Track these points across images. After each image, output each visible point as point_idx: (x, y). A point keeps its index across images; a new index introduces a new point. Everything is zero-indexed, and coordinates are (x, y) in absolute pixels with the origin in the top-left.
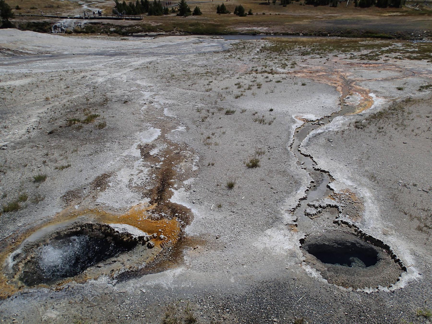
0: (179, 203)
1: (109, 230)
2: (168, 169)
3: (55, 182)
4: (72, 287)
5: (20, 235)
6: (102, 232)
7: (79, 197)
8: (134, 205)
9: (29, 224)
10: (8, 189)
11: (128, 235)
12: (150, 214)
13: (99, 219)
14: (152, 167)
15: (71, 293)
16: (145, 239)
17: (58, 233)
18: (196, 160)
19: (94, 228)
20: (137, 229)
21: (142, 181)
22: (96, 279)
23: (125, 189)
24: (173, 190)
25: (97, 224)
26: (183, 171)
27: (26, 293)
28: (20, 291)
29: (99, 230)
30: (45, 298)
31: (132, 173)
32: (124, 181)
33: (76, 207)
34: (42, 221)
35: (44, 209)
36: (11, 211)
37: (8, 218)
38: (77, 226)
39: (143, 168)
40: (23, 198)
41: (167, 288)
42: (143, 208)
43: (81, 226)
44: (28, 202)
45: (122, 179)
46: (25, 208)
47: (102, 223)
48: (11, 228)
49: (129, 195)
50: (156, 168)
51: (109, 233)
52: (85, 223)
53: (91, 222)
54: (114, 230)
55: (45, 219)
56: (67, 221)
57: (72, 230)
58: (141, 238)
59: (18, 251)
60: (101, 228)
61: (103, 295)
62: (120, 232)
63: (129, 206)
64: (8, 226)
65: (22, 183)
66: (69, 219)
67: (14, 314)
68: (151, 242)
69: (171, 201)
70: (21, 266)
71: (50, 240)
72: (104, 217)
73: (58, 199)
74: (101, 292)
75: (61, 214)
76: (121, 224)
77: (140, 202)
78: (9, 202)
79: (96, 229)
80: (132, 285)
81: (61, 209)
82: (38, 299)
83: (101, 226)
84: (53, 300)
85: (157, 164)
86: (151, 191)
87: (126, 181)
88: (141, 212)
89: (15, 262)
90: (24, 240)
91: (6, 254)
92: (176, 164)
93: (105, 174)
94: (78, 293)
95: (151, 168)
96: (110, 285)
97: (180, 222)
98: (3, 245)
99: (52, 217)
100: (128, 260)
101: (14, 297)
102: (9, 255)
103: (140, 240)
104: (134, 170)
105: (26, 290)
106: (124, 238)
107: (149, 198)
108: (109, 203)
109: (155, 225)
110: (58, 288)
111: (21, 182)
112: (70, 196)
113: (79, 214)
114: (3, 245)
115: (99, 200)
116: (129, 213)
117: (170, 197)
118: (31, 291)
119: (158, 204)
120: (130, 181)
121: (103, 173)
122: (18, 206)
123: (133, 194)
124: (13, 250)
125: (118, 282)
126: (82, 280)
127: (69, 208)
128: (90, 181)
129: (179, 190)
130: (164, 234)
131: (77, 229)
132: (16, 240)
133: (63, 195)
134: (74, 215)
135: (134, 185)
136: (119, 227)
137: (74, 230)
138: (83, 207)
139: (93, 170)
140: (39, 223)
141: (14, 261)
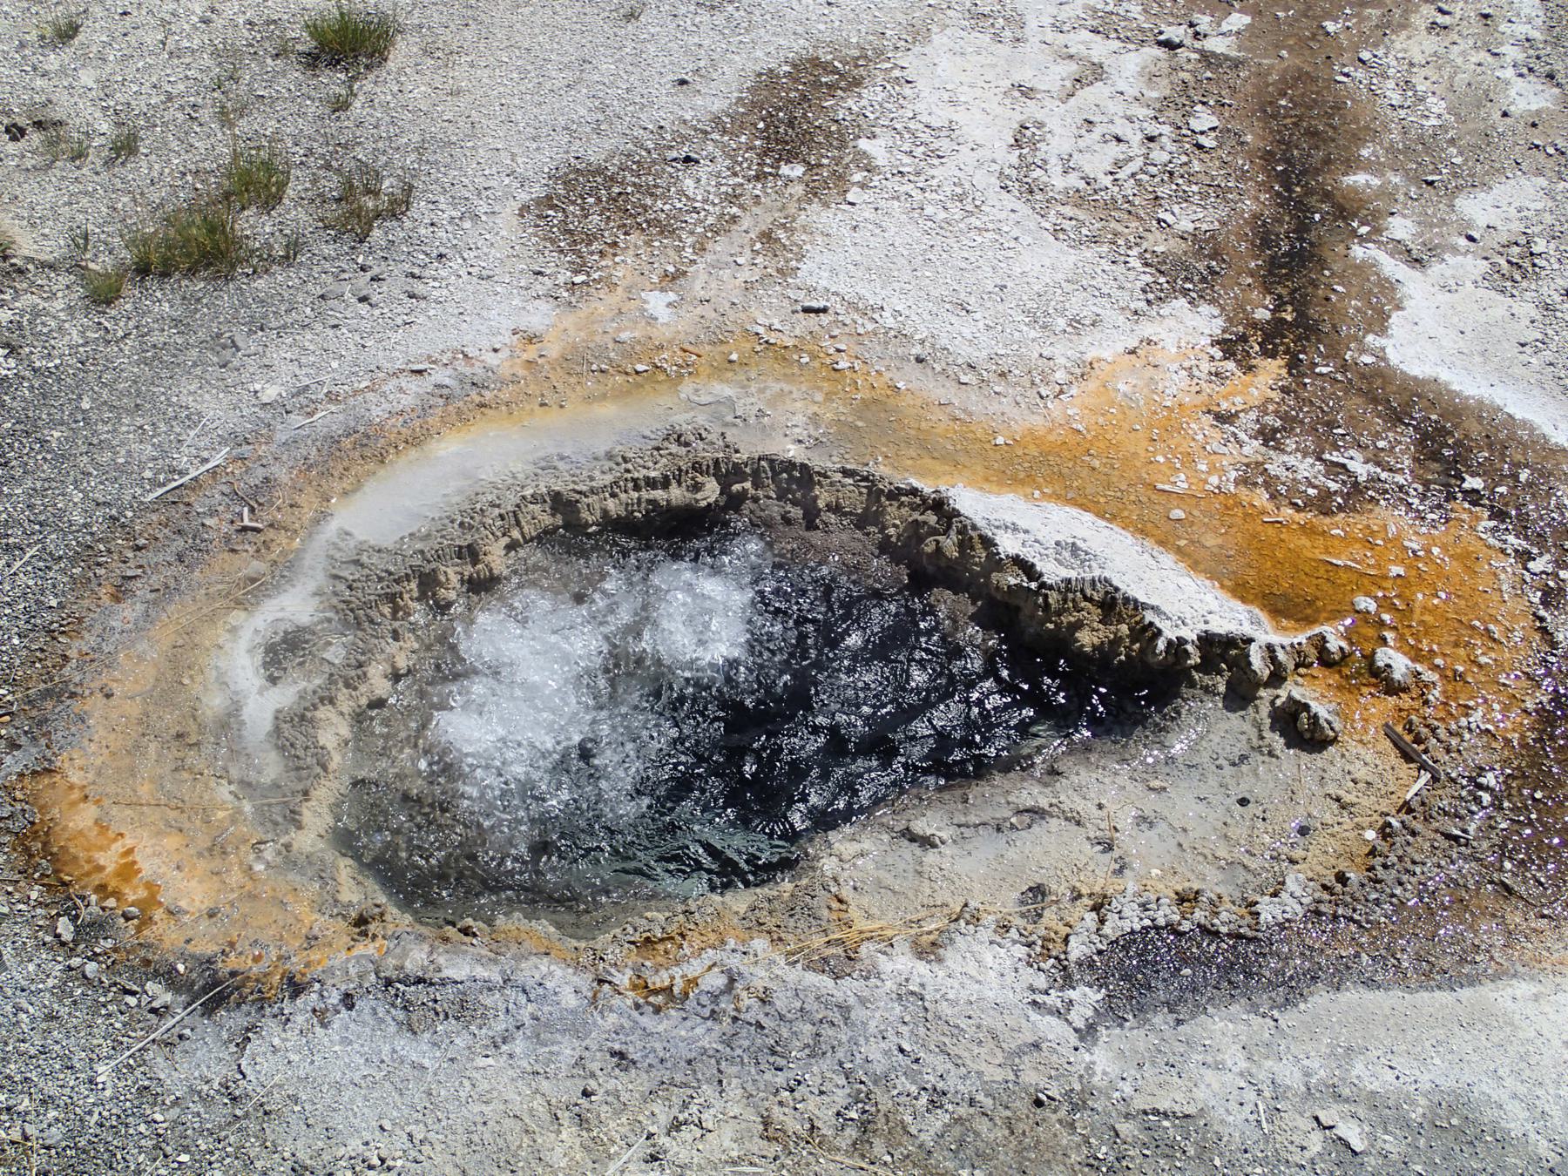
0: (1468, 384)
1: (950, 544)
2: (1301, 76)
3: (460, 75)
4: (759, 984)
5: (281, 473)
6: (885, 547)
7: (666, 230)
8: (1106, 346)
9: (332, 397)
10: (139, 96)
11: (1112, 604)
12: (1253, 448)
13: (846, 432)
14: (1169, 45)
15: (759, 1039)
16: (1257, 661)
17: (558, 502)
18: (1522, 29)
19: (823, 497)
20: (1168, 559)
21: (1114, 150)
22: (929, 950)
23: (1003, 207)
24: (1392, 267)
25: (846, 473)
26: (1436, 105)
27: (420, 981)
28: (367, 949)
29: (861, 522)
30: (567, 1050)
31: (1025, 76)
32: (978, 135)
33: (657, 303)
34: (427, 384)
35: (419, 288)
36: (192, 272)
37: (176, 322)
38: (696, 467)
39: (1100, 49)
40: (256, 183)
41: (1543, 1148)
42: (1175, 384)
43: (728, 474)
44: (295, 214)
45: (960, 117)
46: (287, 260)
47: (886, 472)
48: (215, 409)
49: (1044, 260)
50: (1207, 57)
51: (934, 559)
52: (749, 447)
53: (793, 452)
54: (988, 542)
55: (441, 376)
56: (607, 410)
57: (658, 494)
58: (1221, 650)
59: (296, 605)
60: (881, 513)
61: (1022, 1106)
62: (1052, 572)
63: (1063, 353)
64: (186, 392)
65: (227, 54)
66: (620, 395)
67: (355, 1146)
68: (1316, 696)
69: (1394, 357)
70: (333, 730)
71: (510, 547)
72: (879, 412)
73: (507, 221)
74: (999, 1074)
75: (553, 350)
76: (1029, 497)
77: (1147, 329)
78: (155, 196)
79: (836, 509)
80: (1234, 1058)
81: (543, 305)
82: (519, 1046)
83: (876, 493)
84: (639, 1081)
85: (1204, 22)
86: (1207, 245)
87: (986, 130)
88: (1168, 424)
89: (285, 696)
90: (322, 516)
91: (212, 619)
92: (1364, 40)
93: (816, 62)
94: (814, 1051)
95: (1160, 52)
96: (1050, 1027)
97: (1524, 557)
98: (179, 544)
99: (491, 359)
100: (1143, 821)
101: (334, 998)
102: (233, 630)
103: (1207, 666)
104: (1032, 47)
105: (416, 958)
106: (1078, 625)
107: (1205, 309)
108: (905, 305)
109: (1313, 550)
110: (660, 980)
111: (216, 53)
112: (598, 206)
113: (686, 369)
114: (179, 544)
115: (819, 272)
116: (1074, 409)
117: (1379, 322)
118: (458, 968)
119: (1293, 365)
120: (1023, 138)
121: (800, 47)
122: (237, 242)
123: (1066, 258)
124: (252, 591)
125: (1110, 1012)
126: (818, 941)
127: (603, 304)
128: (718, 96)
129: (1436, 269)
130: (1401, 638)
131: (697, 487)
132: (267, 516)
133: (538, 191)
134: (641, 369)
135: (1059, 182)
136: (1035, 530)
137: (676, 495)
138: (707, 310)
139: (719, 19)
140: (407, 401)
141: (273, 680)
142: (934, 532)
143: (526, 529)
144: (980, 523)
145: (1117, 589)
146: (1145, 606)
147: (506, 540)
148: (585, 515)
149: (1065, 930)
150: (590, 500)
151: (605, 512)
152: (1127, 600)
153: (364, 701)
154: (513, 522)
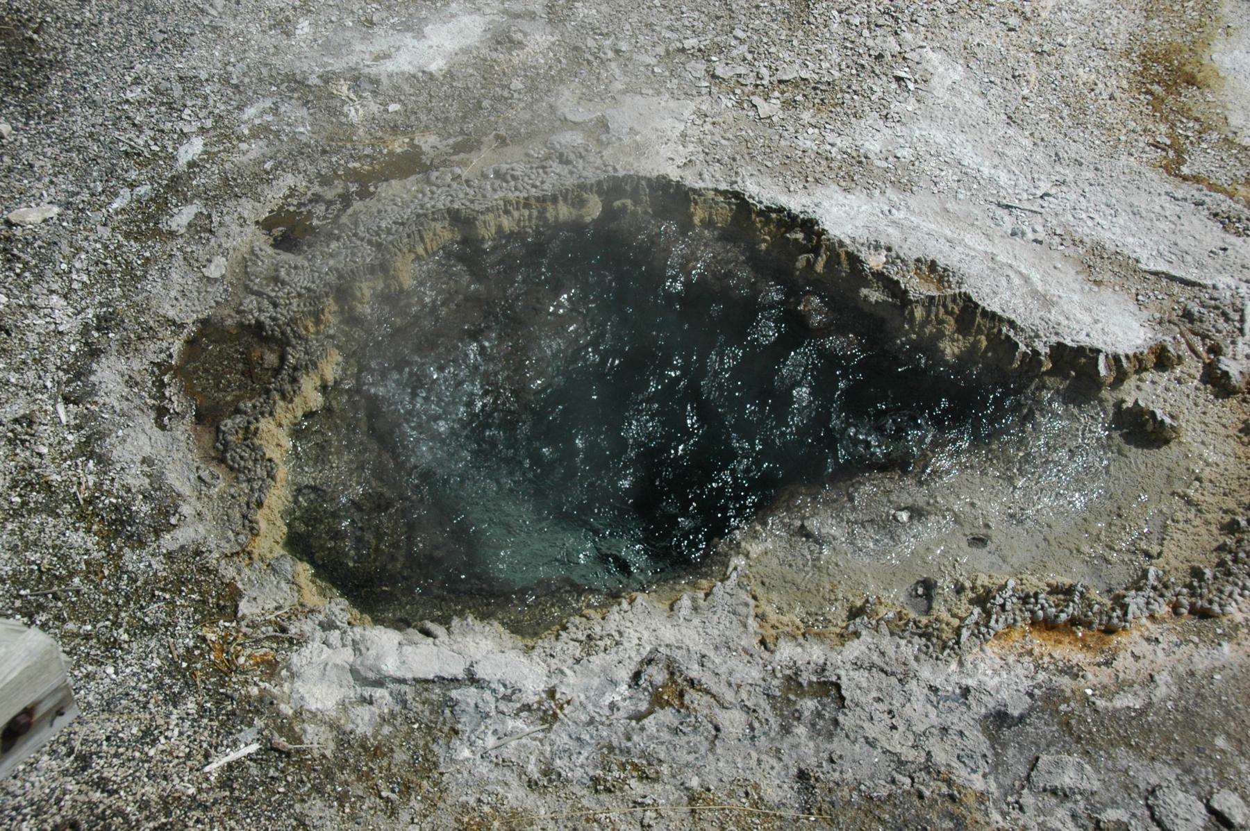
38: (582, 187)
54: (854, 259)
142: (803, 249)
143: (429, 247)
144: (847, 241)
145: (977, 305)
146: (1001, 319)
147: (413, 256)
148: (483, 232)
149: (956, 622)
150: (487, 218)
151: (500, 228)
152: (985, 313)
153: (300, 414)
154: (417, 238)
